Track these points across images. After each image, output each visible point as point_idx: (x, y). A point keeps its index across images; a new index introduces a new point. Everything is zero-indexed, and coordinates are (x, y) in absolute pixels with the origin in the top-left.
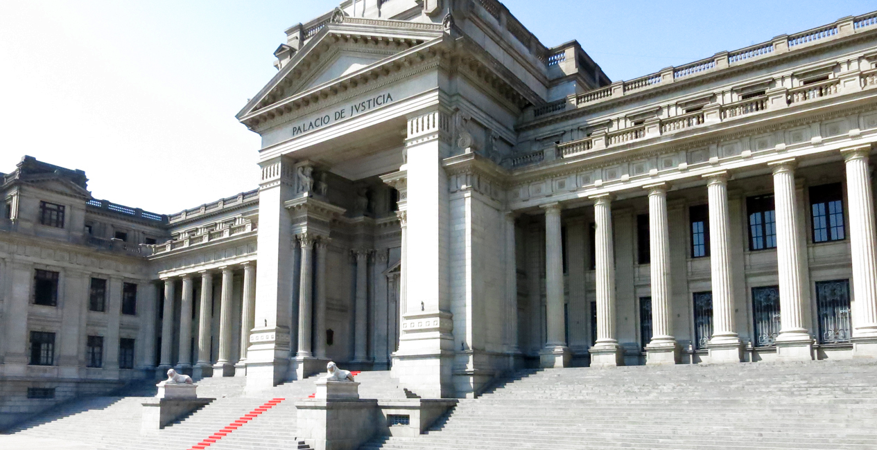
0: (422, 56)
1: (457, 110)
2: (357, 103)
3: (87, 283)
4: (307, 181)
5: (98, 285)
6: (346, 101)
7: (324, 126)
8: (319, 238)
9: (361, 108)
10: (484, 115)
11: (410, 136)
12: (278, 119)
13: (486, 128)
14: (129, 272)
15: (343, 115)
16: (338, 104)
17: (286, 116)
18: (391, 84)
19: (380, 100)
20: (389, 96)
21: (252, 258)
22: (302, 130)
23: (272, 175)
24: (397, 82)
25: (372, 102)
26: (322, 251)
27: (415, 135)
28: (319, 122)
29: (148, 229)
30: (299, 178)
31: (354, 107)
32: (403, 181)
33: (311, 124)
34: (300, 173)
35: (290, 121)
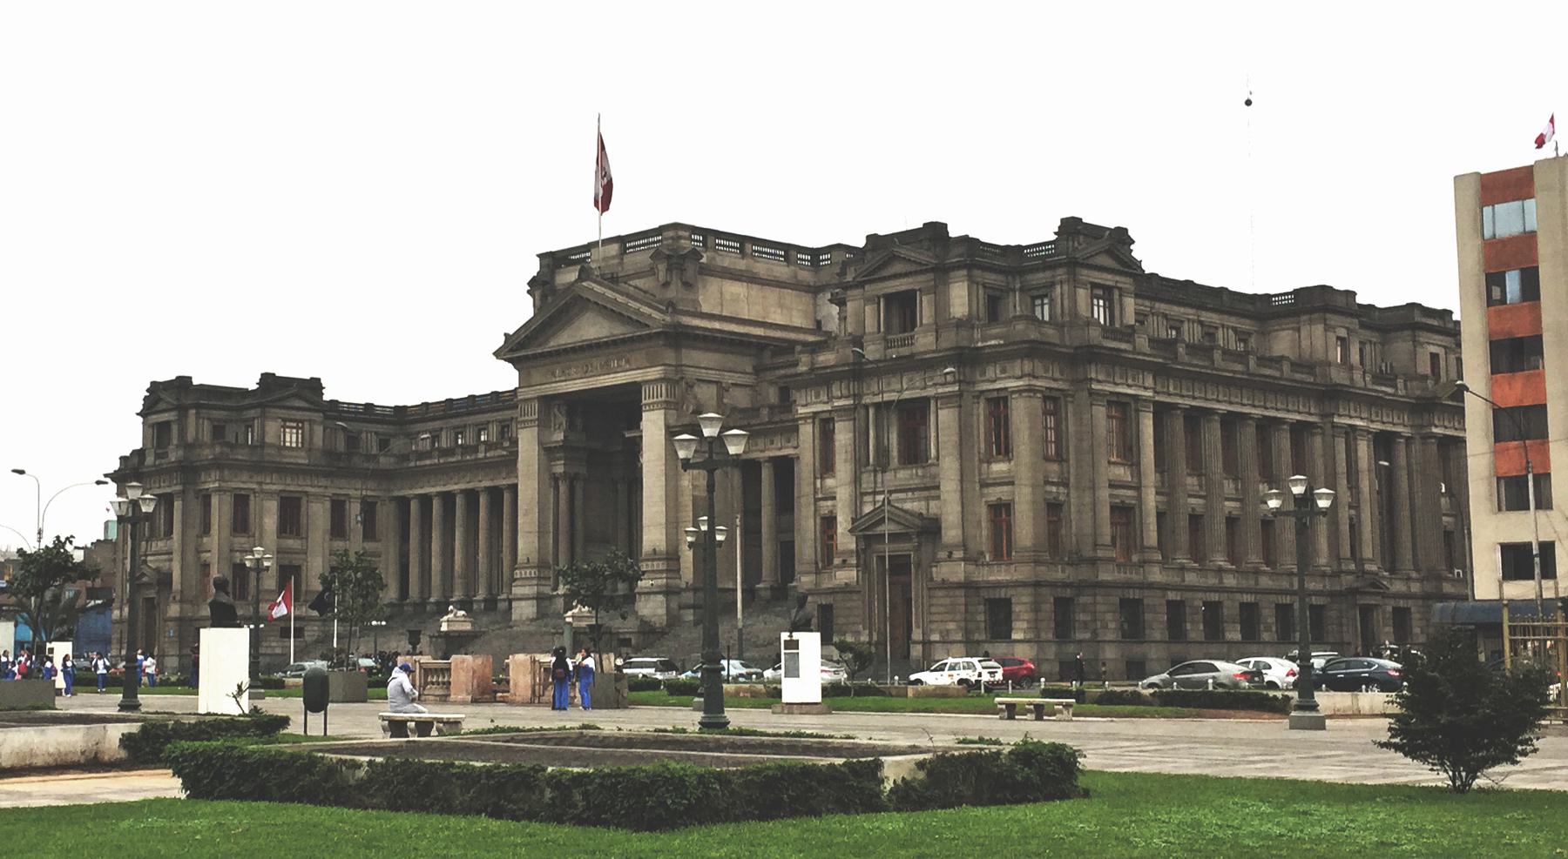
0: (650, 337)
1: (682, 378)
3: (328, 505)
4: (563, 420)
5: (338, 508)
8: (576, 474)
10: (714, 372)
11: (644, 402)
13: (716, 382)
14: (370, 490)
21: (510, 481)
26: (579, 487)
27: (647, 401)
29: (380, 428)
30: (555, 415)
32: (641, 437)
34: (556, 410)
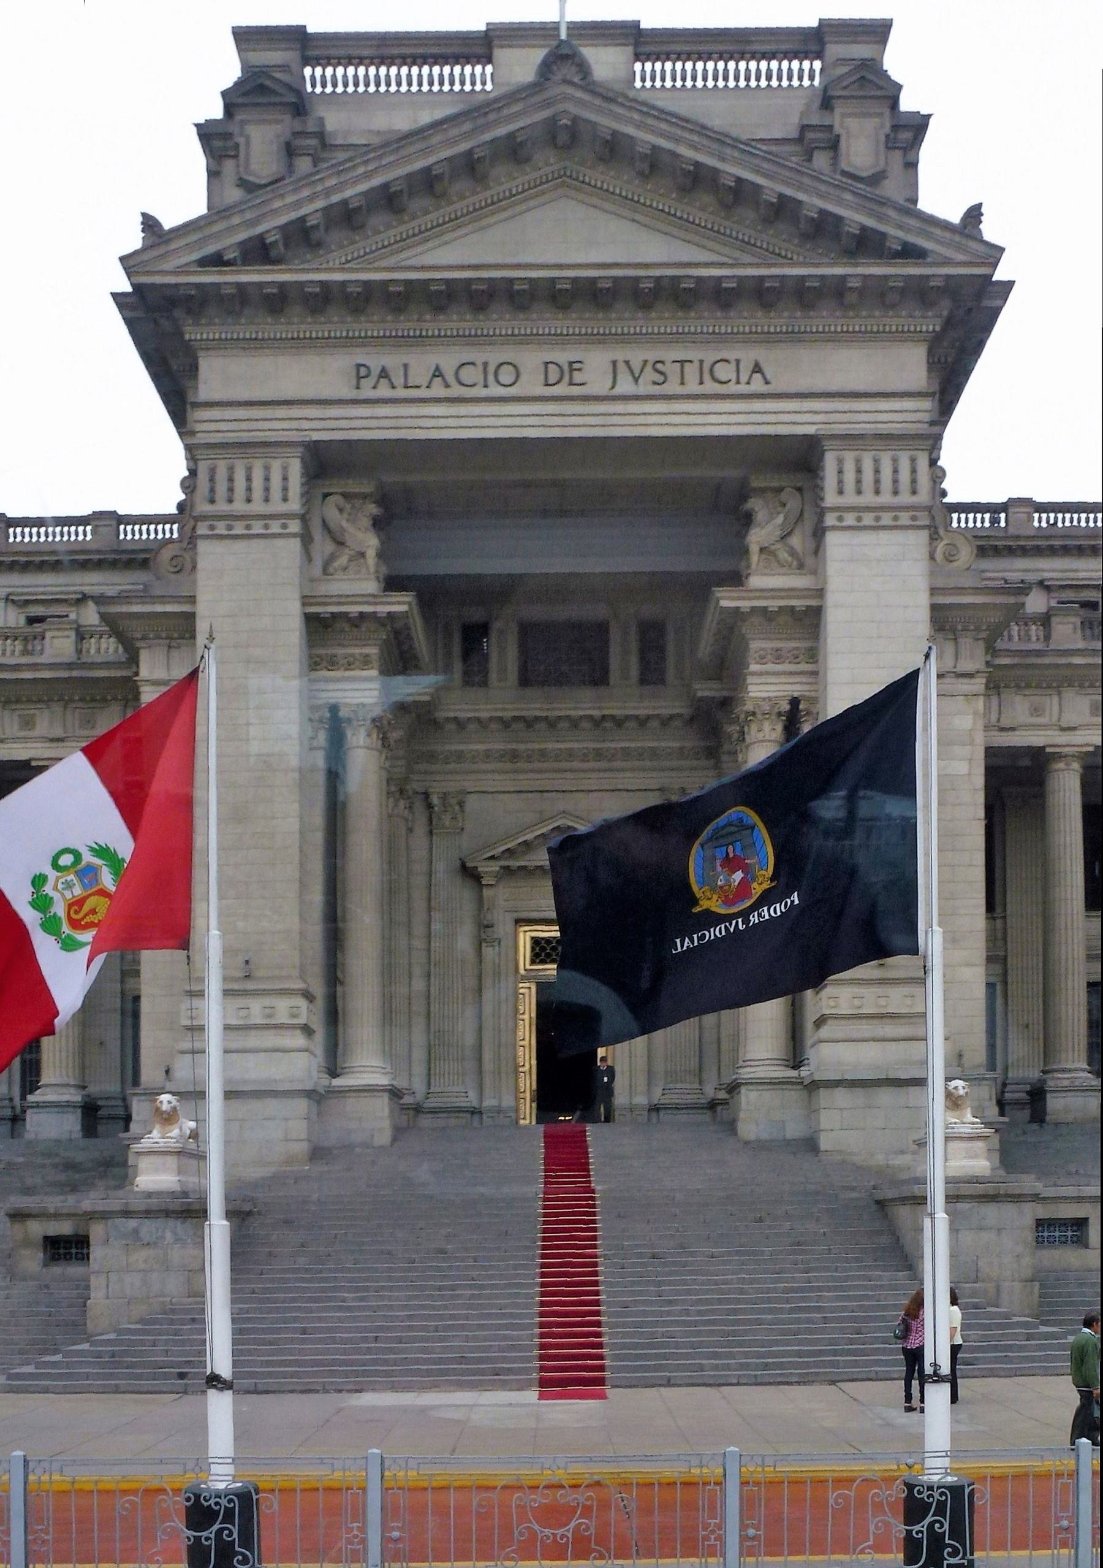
2: (637, 356)
6: (600, 340)
7: (496, 391)
9: (649, 375)
12: (297, 324)
15: (578, 377)
16: (560, 339)
17: (335, 324)
18: (769, 339)
19: (724, 372)
20: (757, 369)
22: (399, 380)
23: (258, 493)
24: (794, 337)
25: (691, 371)
28: (467, 374)
31: (621, 367)
33: (438, 373)
35: (348, 342)
